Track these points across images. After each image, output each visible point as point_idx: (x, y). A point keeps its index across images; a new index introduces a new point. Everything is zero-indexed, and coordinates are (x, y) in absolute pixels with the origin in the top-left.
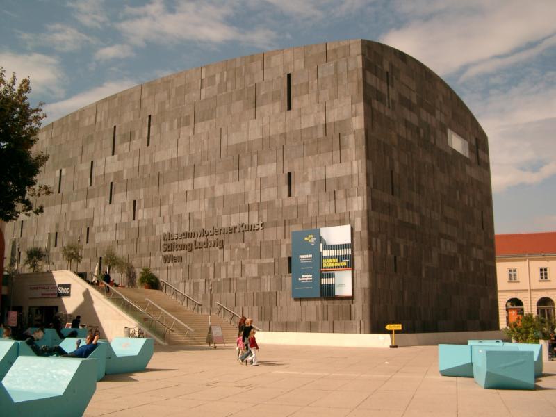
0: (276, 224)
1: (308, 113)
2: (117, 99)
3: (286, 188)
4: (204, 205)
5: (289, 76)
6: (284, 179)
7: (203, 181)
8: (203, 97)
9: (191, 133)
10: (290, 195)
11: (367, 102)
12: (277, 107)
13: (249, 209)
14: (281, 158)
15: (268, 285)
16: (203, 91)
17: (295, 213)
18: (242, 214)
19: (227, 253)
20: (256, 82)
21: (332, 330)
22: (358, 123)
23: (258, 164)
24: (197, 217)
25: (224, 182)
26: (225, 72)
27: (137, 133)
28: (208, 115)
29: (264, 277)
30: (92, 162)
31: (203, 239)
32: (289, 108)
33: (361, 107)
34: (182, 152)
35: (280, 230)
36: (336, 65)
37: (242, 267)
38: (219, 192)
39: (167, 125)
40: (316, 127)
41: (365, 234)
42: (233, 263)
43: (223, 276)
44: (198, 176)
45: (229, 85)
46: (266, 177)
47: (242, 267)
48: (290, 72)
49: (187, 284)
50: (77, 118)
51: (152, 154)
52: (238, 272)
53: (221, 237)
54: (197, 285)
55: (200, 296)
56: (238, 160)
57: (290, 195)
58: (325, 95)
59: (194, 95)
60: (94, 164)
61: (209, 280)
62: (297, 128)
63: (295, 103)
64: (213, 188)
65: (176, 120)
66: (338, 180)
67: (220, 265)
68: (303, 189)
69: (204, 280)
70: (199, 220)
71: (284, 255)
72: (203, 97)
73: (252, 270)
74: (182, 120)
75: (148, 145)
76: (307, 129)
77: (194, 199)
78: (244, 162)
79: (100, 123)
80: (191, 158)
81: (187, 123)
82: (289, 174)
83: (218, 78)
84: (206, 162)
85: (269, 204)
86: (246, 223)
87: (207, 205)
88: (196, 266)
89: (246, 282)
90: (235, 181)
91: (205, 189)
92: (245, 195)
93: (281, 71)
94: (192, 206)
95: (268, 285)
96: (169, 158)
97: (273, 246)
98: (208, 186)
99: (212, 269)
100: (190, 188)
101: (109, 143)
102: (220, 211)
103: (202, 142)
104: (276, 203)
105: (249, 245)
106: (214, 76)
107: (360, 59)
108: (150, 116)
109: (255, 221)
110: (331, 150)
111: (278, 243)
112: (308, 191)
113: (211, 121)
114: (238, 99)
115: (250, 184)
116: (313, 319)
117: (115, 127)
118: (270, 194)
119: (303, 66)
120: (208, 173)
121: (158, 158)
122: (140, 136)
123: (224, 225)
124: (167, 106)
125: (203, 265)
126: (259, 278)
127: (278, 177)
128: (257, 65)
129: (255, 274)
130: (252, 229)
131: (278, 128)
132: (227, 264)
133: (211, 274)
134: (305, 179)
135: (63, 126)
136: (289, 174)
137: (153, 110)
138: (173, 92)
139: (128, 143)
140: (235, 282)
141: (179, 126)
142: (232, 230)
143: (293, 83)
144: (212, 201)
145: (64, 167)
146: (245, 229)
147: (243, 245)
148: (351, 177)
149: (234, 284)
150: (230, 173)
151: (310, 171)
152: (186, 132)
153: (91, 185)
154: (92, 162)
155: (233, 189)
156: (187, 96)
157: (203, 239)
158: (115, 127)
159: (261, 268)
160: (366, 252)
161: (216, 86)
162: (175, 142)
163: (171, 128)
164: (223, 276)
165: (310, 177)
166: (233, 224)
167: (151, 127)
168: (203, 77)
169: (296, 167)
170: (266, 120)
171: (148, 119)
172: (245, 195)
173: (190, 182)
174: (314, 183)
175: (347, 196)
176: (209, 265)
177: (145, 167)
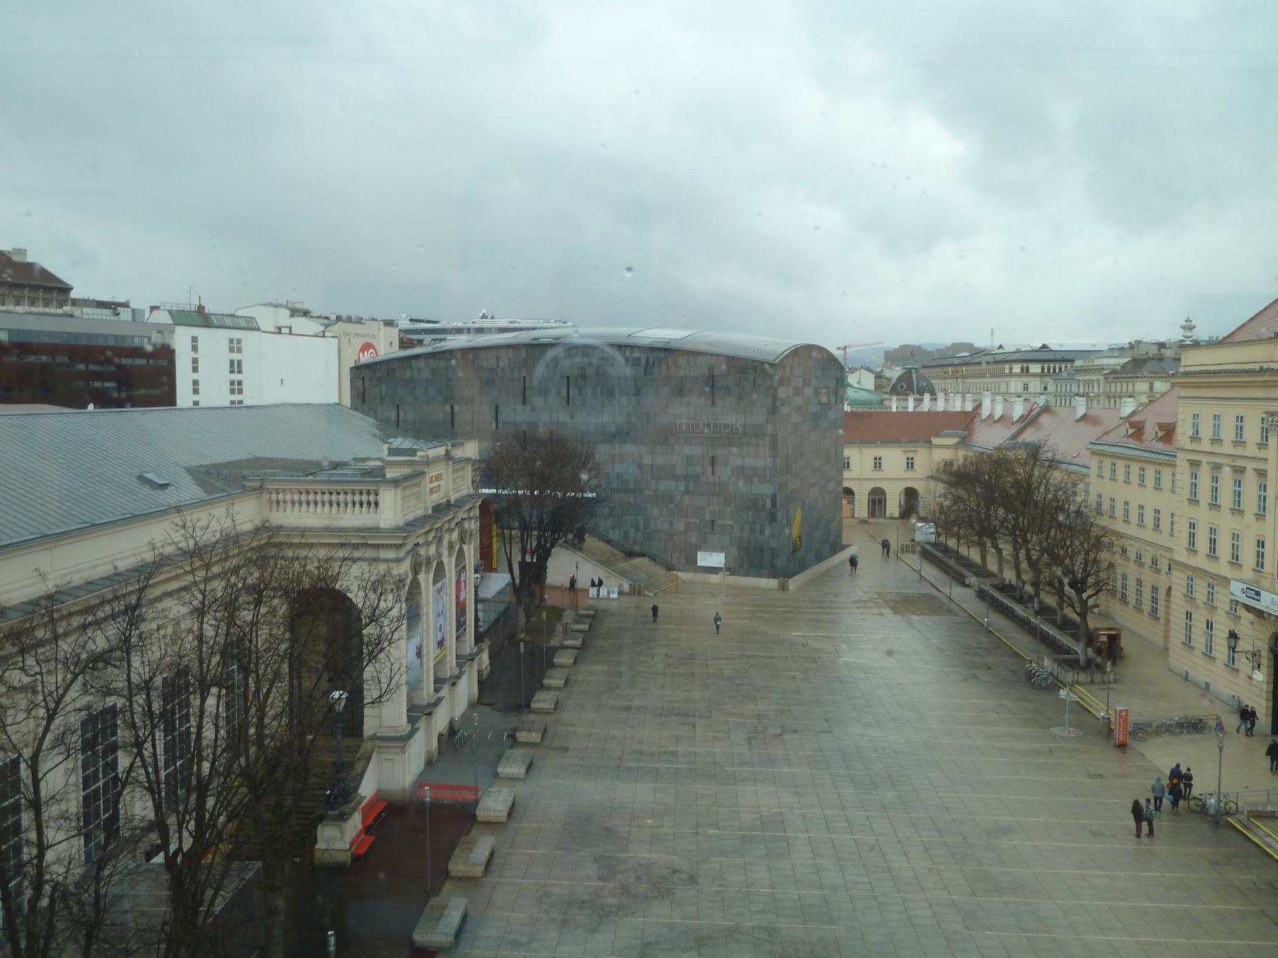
3: (709, 471)
10: (713, 473)
13: (676, 478)
21: (747, 574)
27: (553, 390)
30: (497, 407)
32: (713, 404)
34: (605, 419)
36: (754, 379)
37: (671, 523)
38: (647, 460)
39: (589, 391)
42: (662, 519)
47: (671, 523)
48: (715, 374)
49: (617, 531)
52: (667, 526)
54: (626, 535)
57: (713, 473)
60: (501, 409)
61: (639, 530)
64: (641, 456)
65: (599, 389)
66: (754, 469)
68: (723, 473)
69: (634, 530)
71: (708, 517)
74: (605, 389)
82: (713, 457)
94: (618, 468)
99: (641, 522)
100: (617, 452)
102: (649, 477)
108: (568, 378)
112: (729, 473)
117: (524, 378)
118: (698, 469)
128: (682, 360)
129: (683, 529)
133: (641, 526)
134: (727, 463)
136: (713, 457)
147: (671, 506)
148: (765, 468)
154: (497, 407)
155: (661, 460)
158: (524, 378)
159: (688, 525)
171: (566, 379)
173: (617, 447)
176: (638, 518)
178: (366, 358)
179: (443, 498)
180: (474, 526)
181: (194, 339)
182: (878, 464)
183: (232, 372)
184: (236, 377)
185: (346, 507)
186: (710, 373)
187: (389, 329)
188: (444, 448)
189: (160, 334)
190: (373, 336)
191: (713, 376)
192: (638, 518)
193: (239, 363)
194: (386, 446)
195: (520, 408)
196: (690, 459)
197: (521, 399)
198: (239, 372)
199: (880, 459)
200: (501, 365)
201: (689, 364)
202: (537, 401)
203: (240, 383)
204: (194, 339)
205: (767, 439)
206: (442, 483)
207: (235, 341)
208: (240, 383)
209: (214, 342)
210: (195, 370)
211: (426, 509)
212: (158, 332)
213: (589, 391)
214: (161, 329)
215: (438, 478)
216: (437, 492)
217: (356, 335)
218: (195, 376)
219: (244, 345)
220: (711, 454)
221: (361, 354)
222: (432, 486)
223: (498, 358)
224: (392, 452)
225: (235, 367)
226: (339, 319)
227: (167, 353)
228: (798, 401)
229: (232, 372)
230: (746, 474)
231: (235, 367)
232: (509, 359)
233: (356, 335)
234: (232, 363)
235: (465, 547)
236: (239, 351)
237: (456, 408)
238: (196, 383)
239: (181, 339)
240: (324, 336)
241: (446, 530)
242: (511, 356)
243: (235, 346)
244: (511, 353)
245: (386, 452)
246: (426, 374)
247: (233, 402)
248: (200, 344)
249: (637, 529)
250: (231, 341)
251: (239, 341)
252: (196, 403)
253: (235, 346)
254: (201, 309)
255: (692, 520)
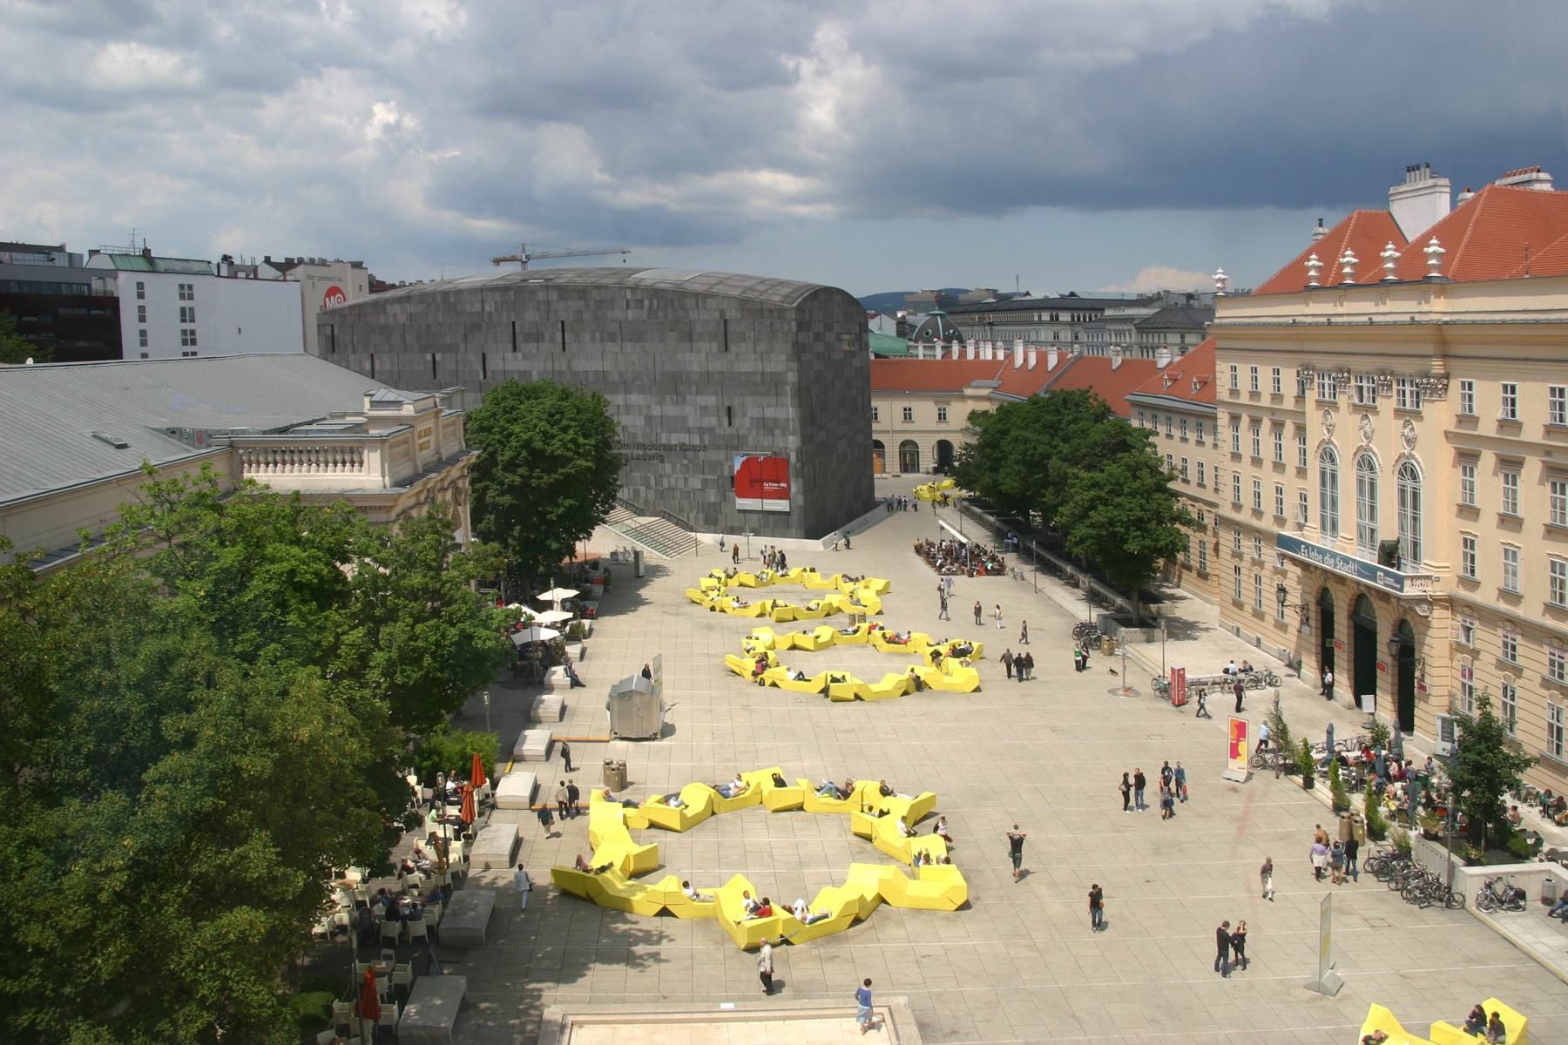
0: (718, 448)
1: (746, 362)
2: (512, 293)
3: (726, 420)
4: (640, 421)
5: (725, 321)
6: (723, 412)
7: (635, 399)
8: (630, 318)
9: (618, 350)
10: (730, 424)
11: (799, 359)
12: (714, 347)
13: (689, 431)
14: (720, 393)
15: (712, 496)
16: (629, 312)
17: (736, 442)
18: (682, 435)
19: (668, 468)
20: (692, 318)
22: (792, 377)
23: (698, 393)
24: (632, 430)
25: (661, 403)
26: (655, 301)
27: (547, 336)
28: (638, 337)
29: (707, 490)
30: (484, 355)
31: (641, 452)
32: (726, 350)
33: (794, 366)
34: (608, 366)
35: (721, 455)
36: (771, 323)
37: (686, 480)
38: (656, 411)
40: (754, 373)
41: (799, 465)
43: (666, 484)
44: (631, 393)
45: (661, 314)
46: (705, 407)
47: (686, 480)
48: (727, 318)
50: (452, 300)
51: (569, 362)
52: (681, 484)
53: (662, 453)
55: (642, 501)
56: (675, 385)
58: (762, 347)
59: (618, 314)
60: (488, 357)
61: (650, 488)
62: (735, 370)
63: (733, 347)
64: (649, 407)
65: (598, 335)
66: (776, 420)
67: (661, 476)
68: (743, 423)
70: (635, 435)
72: (630, 318)
73: (696, 483)
75: (564, 349)
76: (746, 373)
77: (628, 413)
78: (682, 388)
79: (490, 314)
80: (621, 374)
81: (612, 338)
82: (729, 408)
83: (646, 303)
84: (638, 382)
85: (711, 430)
86: (687, 442)
87: (643, 422)
88: (635, 474)
89: (689, 492)
90: (673, 404)
91: (640, 406)
92: (685, 419)
93: (717, 315)
95: (712, 496)
96: (594, 369)
97: (715, 466)
98: (642, 403)
101: (508, 338)
102: (659, 430)
103: (633, 363)
104: (717, 431)
105: (691, 461)
106: (641, 301)
107: (794, 324)
108: (563, 322)
109: (697, 442)
110: (768, 395)
111: (720, 464)
112: (748, 424)
113: (642, 344)
114: (673, 331)
115: (688, 410)
116: (756, 525)
117: (514, 323)
118: (711, 421)
119: (739, 316)
120: (642, 392)
121: (579, 365)
122: (553, 340)
123: (664, 441)
124: (585, 317)
125: (643, 474)
126: (702, 490)
127: (718, 408)
128: (690, 302)
129: (699, 487)
130: (695, 449)
131: (717, 366)
132: (669, 476)
134: (744, 415)
135: (429, 304)
136: (729, 408)
137: (568, 317)
138: (592, 304)
139: (536, 344)
140: (678, 492)
141: (602, 340)
142: (669, 448)
143: (731, 329)
144: (649, 419)
145: (439, 352)
146: (684, 448)
147: (685, 462)
148: (787, 420)
149: (678, 494)
150: (668, 397)
151: (752, 409)
152: (612, 347)
153: (485, 377)
154: (484, 355)
155: (671, 411)
156: (609, 313)
157: (641, 452)
158: (514, 323)
159: (705, 482)
160: (801, 480)
161: (645, 311)
162: (599, 355)
163: (593, 341)
164: (666, 484)
165: (749, 414)
166: (673, 442)
167: (566, 334)
168: (629, 296)
169: (736, 402)
170: (703, 356)
171: (560, 324)
172: (685, 419)
174: (752, 419)
175: (783, 434)
176: (649, 475)
177: (561, 373)
178: (333, 303)
179: (433, 456)
180: (465, 484)
181: (140, 285)
182: (908, 415)
183: (184, 321)
184: (188, 326)
185: (353, 466)
186: (721, 317)
187: (357, 271)
188: (431, 400)
189: (101, 281)
190: (340, 280)
191: (725, 321)
192: (649, 475)
193: (192, 310)
194: (367, 400)
195: (510, 355)
196: (704, 409)
197: (510, 346)
198: (193, 321)
199: (910, 410)
200: (487, 308)
201: (697, 307)
202: (530, 347)
203: (193, 332)
204: (140, 285)
205: (788, 388)
206: (432, 438)
207: (186, 287)
208: (193, 332)
209: (163, 291)
210: (142, 319)
211: (416, 467)
212: (100, 278)
213: (587, 337)
214: (102, 274)
215: (427, 432)
216: (427, 448)
217: (321, 278)
218: (143, 326)
219: (196, 291)
220: (727, 404)
221: (327, 299)
222: (421, 441)
223: (483, 302)
224: (375, 404)
225: (186, 315)
226: (301, 261)
227: (112, 303)
228: (820, 347)
229: (184, 321)
230: (767, 426)
231: (186, 315)
232: (496, 303)
233: (321, 278)
234: (183, 310)
235: (460, 509)
236: (191, 297)
237: (438, 357)
238: (143, 333)
239: (124, 287)
240: (285, 280)
241: (439, 491)
242: (498, 300)
243: (186, 292)
244: (498, 296)
245: (367, 405)
246: (402, 319)
247: (185, 354)
248: (147, 291)
249: (648, 487)
250: (182, 286)
251: (190, 287)
252: (144, 355)
253: (186, 292)
254: (146, 254)
255: (709, 477)
